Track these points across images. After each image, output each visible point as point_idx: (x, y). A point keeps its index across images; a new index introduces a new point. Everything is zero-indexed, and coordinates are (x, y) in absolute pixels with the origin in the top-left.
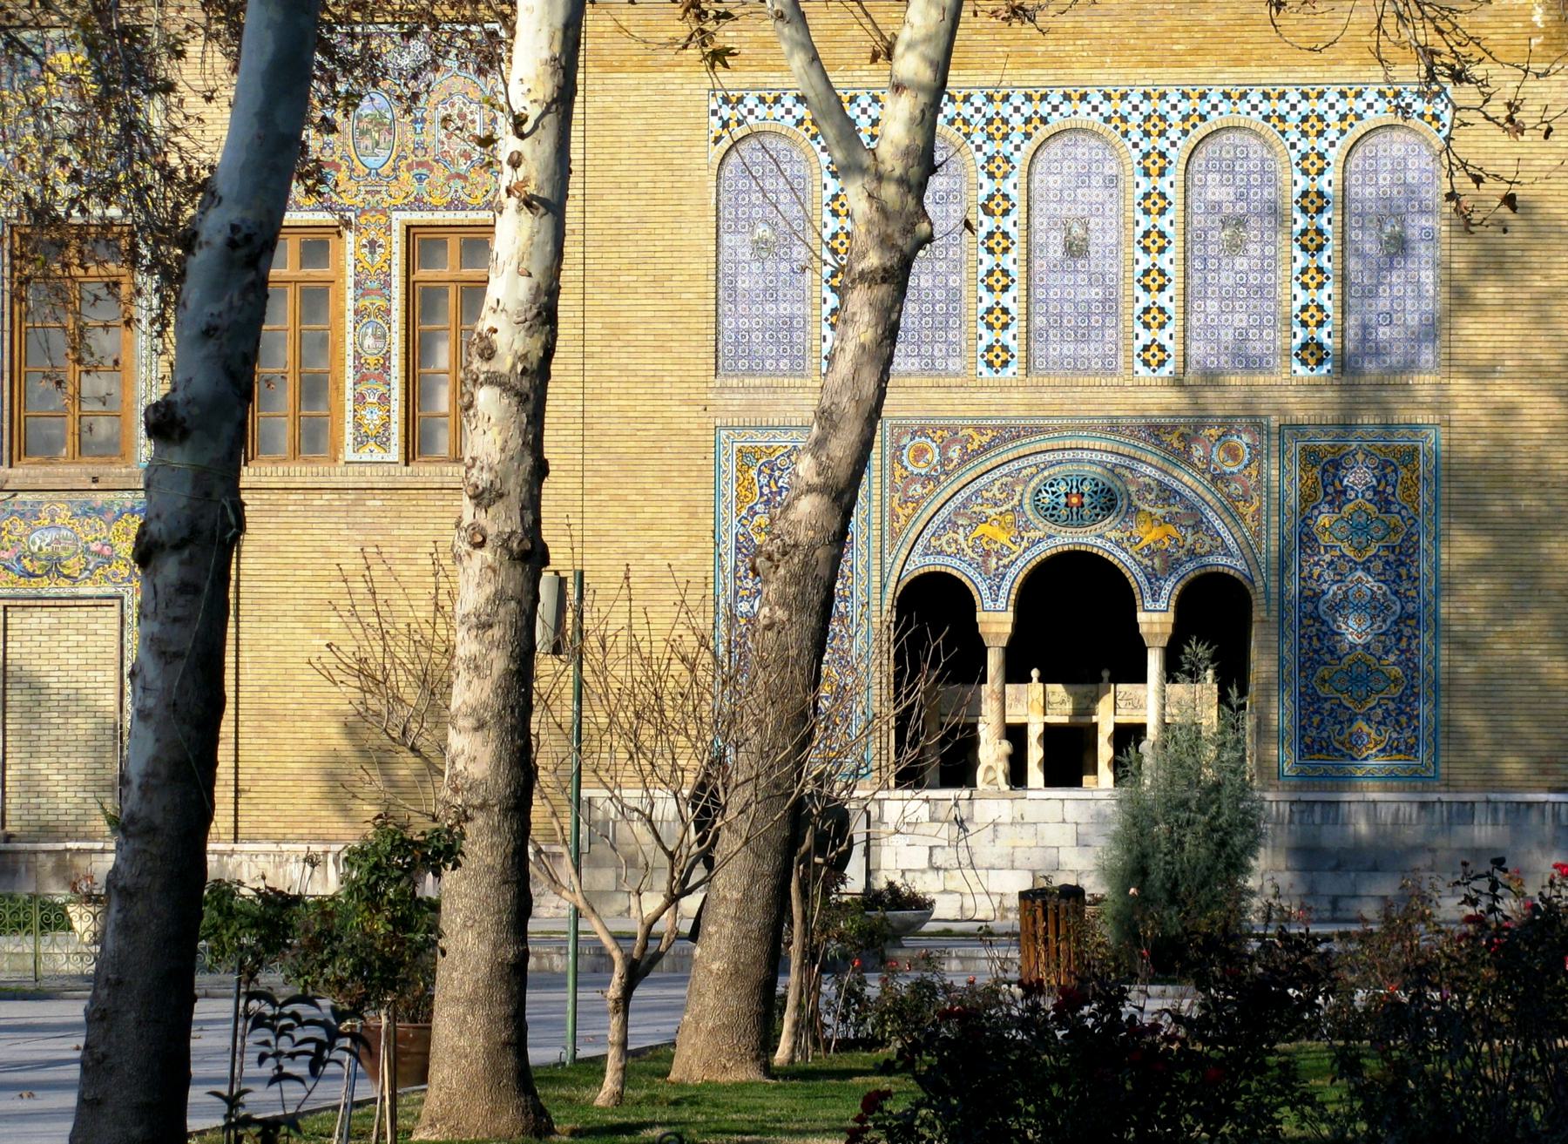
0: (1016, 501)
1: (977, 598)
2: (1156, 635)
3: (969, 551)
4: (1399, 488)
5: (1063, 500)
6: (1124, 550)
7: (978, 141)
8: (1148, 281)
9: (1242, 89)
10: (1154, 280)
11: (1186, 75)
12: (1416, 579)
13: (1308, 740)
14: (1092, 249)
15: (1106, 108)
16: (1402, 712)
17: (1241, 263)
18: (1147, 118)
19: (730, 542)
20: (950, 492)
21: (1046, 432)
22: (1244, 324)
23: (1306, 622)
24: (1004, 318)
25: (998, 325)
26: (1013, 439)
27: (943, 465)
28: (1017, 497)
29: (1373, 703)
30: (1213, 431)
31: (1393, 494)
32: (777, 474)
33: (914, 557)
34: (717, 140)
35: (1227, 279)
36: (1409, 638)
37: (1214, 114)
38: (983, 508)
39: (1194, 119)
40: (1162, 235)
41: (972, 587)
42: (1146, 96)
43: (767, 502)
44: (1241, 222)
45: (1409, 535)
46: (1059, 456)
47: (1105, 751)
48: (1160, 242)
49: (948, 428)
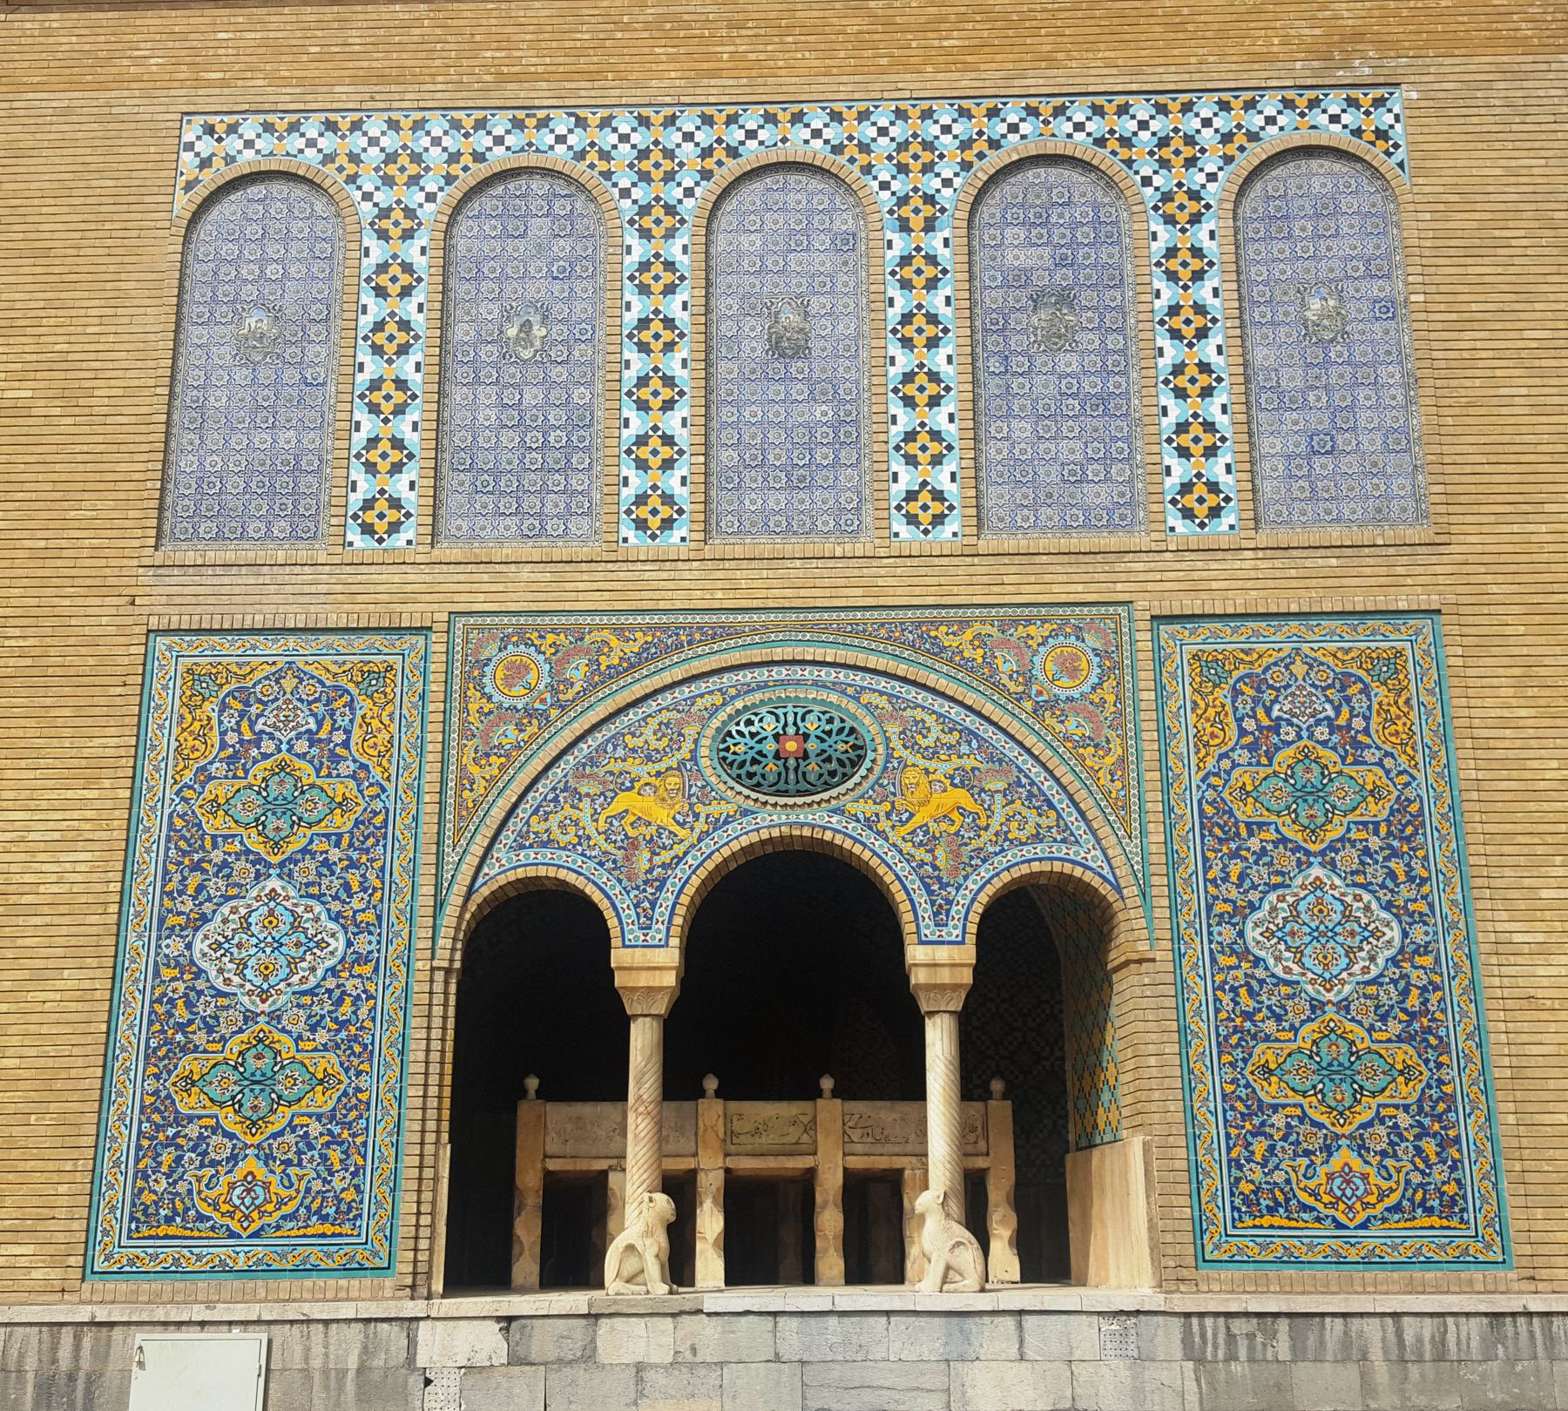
0: (685, 753)
2: (941, 988)
4: (1375, 719)
5: (770, 747)
7: (625, 183)
8: (910, 390)
9: (1058, 101)
10: (921, 389)
11: (966, 83)
12: (1424, 881)
13: (1245, 1187)
14: (816, 345)
15: (833, 133)
16: (1424, 1133)
17: (1068, 362)
18: (903, 146)
19: (156, 825)
21: (739, 634)
22: (1078, 457)
23: (1223, 960)
24: (666, 452)
25: (655, 462)
26: (679, 647)
27: (554, 690)
28: (688, 746)
29: (1368, 1115)
30: (1032, 630)
31: (1366, 732)
32: (254, 709)
33: (499, 852)
34: (189, 186)
35: (1045, 387)
36: (1424, 989)
37: (1013, 138)
38: (628, 765)
39: (981, 146)
40: (933, 319)
41: (604, 905)
42: (900, 114)
43: (232, 760)
44: (1065, 299)
45: (1402, 804)
46: (762, 675)
47: (830, 1222)
48: (931, 331)
49: (566, 630)
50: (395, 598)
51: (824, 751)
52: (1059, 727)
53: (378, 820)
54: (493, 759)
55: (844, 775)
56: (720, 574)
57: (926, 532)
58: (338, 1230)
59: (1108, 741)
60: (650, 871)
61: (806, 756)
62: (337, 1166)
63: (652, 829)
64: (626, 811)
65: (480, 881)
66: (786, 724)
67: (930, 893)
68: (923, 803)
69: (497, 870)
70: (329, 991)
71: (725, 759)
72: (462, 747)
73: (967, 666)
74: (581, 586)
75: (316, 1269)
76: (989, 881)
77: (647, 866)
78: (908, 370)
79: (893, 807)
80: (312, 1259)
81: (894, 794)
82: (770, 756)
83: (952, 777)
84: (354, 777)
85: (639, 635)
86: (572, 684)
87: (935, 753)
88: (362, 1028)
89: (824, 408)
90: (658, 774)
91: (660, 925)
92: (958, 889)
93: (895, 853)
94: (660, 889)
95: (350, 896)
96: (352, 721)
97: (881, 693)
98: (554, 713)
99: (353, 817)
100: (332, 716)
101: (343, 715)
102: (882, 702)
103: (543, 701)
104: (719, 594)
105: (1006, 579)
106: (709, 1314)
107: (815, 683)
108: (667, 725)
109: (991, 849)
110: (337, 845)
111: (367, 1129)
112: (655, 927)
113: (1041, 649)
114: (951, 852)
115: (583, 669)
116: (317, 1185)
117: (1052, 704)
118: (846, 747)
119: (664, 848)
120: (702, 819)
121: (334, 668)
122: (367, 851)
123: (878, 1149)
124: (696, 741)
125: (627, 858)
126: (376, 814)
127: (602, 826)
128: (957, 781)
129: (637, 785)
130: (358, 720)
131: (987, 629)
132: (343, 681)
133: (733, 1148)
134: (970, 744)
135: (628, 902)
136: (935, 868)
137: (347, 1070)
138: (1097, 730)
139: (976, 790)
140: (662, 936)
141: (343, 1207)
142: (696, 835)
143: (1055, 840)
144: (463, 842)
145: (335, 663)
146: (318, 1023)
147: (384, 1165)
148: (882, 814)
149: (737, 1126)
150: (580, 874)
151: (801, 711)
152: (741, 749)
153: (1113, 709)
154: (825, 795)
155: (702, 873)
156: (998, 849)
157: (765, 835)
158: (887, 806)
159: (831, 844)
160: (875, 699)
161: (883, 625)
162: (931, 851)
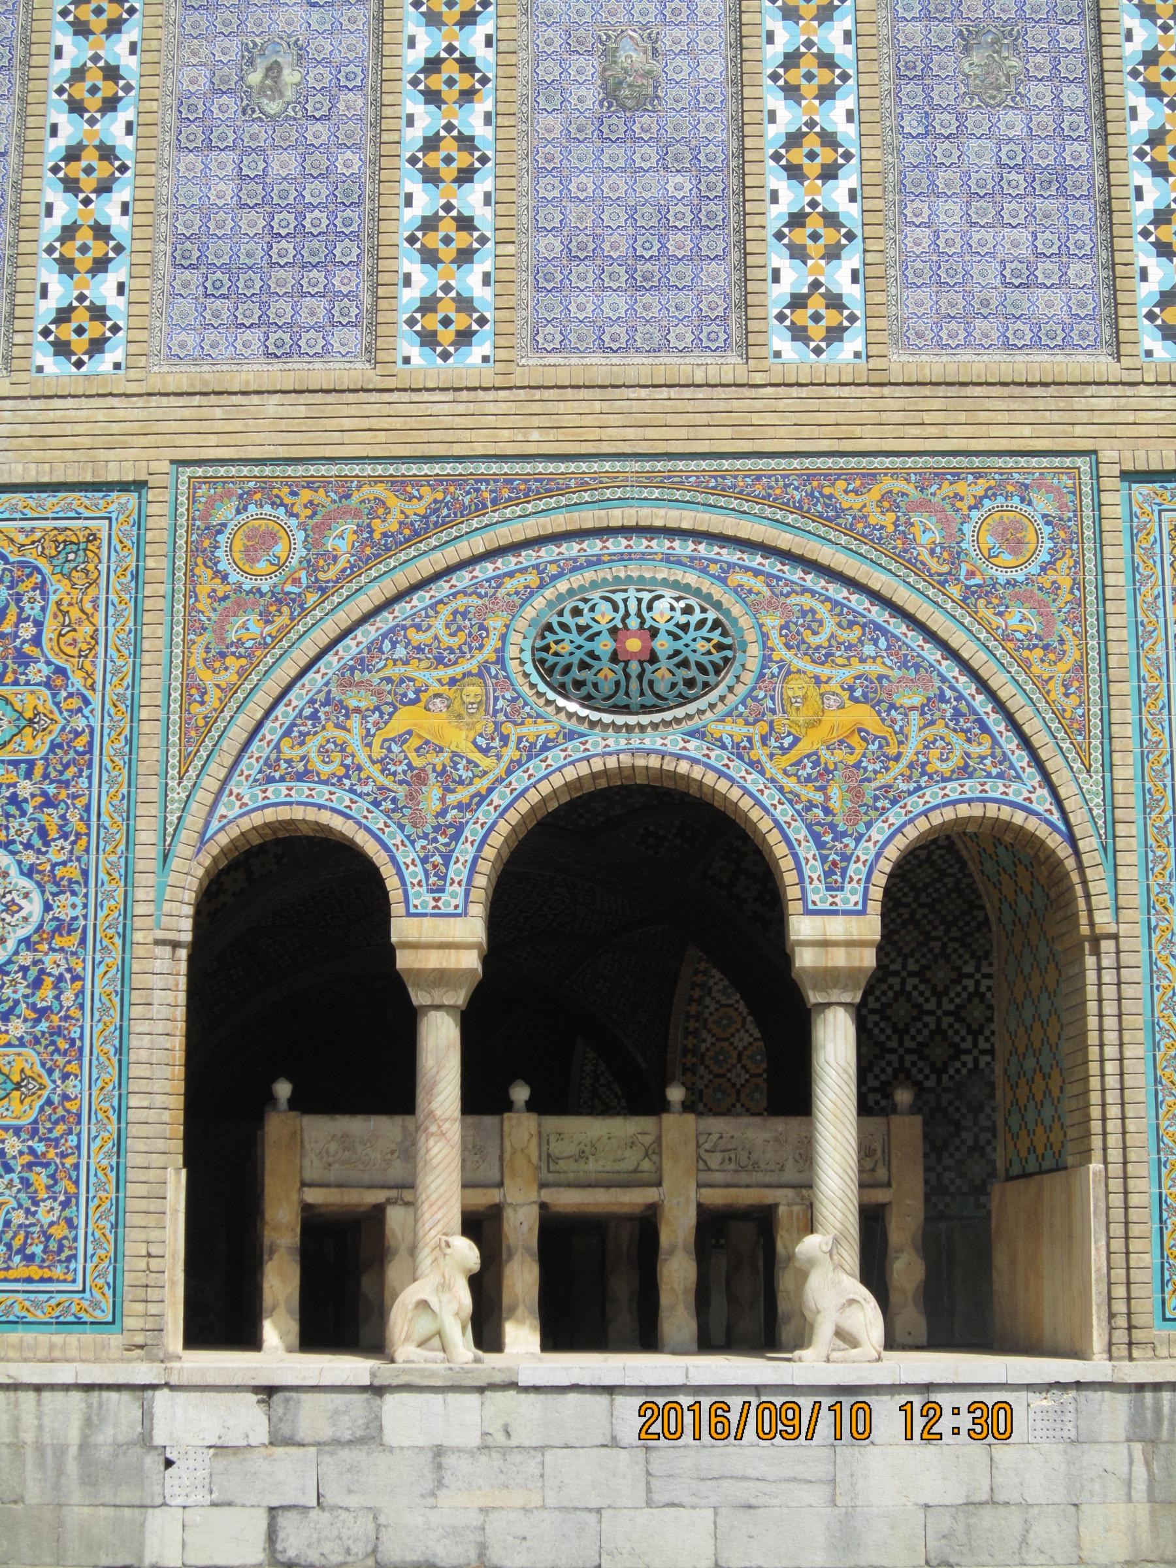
0: (488, 653)
1: (392, 882)
3: (374, 771)
5: (605, 645)
6: (755, 765)
17: (1013, 122)
20: (330, 629)
21: (563, 491)
24: (462, 240)
25: (447, 253)
28: (492, 643)
30: (961, 487)
33: (239, 785)
41: (380, 858)
46: (594, 547)
48: (824, 76)
50: (99, 442)
51: (677, 653)
52: (999, 621)
53: (80, 744)
54: (230, 661)
55: (706, 684)
56: (536, 408)
57: (818, 351)
58: (47, 1274)
59: (1062, 641)
60: (442, 813)
61: (653, 658)
62: (43, 1195)
63: (445, 757)
64: (410, 732)
65: (215, 825)
66: (627, 614)
67: (820, 845)
68: (813, 724)
69: (237, 811)
70: (24, 969)
71: (543, 661)
72: (188, 645)
73: (872, 537)
74: (347, 424)
75: (21, 1322)
76: (899, 830)
77: (437, 806)
78: (793, 129)
79: (772, 728)
80: (17, 1308)
81: (773, 711)
82: (605, 658)
83: (851, 689)
84: (47, 684)
85: (425, 490)
86: (335, 559)
87: (827, 655)
88: (67, 1018)
89: (679, 179)
90: (453, 681)
91: (455, 887)
92: (858, 840)
93: (774, 791)
94: (456, 838)
95: (47, 844)
96: (43, 609)
97: (757, 573)
98: (312, 598)
99: (48, 739)
100: (18, 602)
101: (32, 601)
102: (758, 584)
103: (296, 582)
104: (535, 435)
105: (927, 418)
106: (527, 1389)
107: (667, 559)
108: (464, 615)
109: (904, 786)
110: (29, 775)
111: (78, 1147)
112: (449, 889)
113: (975, 514)
114: (849, 790)
115: (350, 537)
116: (18, 1218)
117: (987, 590)
118: (709, 646)
119: (461, 782)
120: (512, 744)
121: (21, 538)
122: (67, 784)
123: (744, 1178)
124: (503, 637)
125: (411, 796)
126: (78, 734)
127: (377, 753)
128: (858, 693)
129: (424, 697)
130: (52, 608)
131: (900, 485)
132: (31, 556)
133: (551, 1177)
134: (875, 642)
135: (413, 855)
136: (827, 811)
137: (50, 1072)
138: (1048, 625)
139: (884, 706)
140: (460, 900)
141: (53, 1246)
142: (503, 765)
143: (989, 775)
144: (192, 773)
145: (22, 530)
146: (11, 1010)
147: (102, 1194)
148: (757, 738)
149: (556, 1148)
150: (348, 817)
151: (646, 596)
152: (566, 648)
153: (1069, 597)
154: (680, 712)
155: (513, 817)
156: (912, 786)
157: (597, 765)
158: (762, 728)
159: (687, 778)
160: (748, 580)
161: (758, 478)
162: (822, 789)
